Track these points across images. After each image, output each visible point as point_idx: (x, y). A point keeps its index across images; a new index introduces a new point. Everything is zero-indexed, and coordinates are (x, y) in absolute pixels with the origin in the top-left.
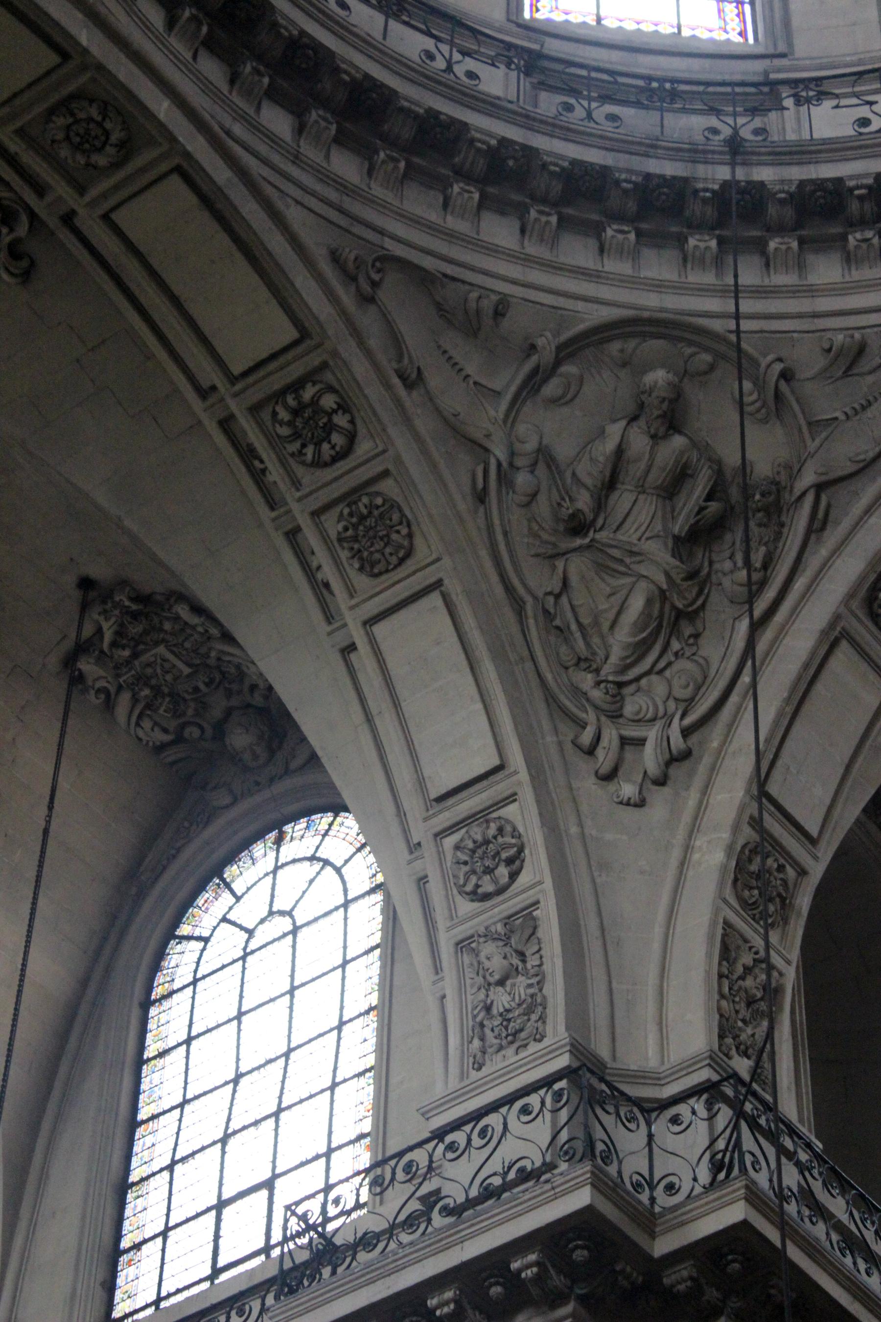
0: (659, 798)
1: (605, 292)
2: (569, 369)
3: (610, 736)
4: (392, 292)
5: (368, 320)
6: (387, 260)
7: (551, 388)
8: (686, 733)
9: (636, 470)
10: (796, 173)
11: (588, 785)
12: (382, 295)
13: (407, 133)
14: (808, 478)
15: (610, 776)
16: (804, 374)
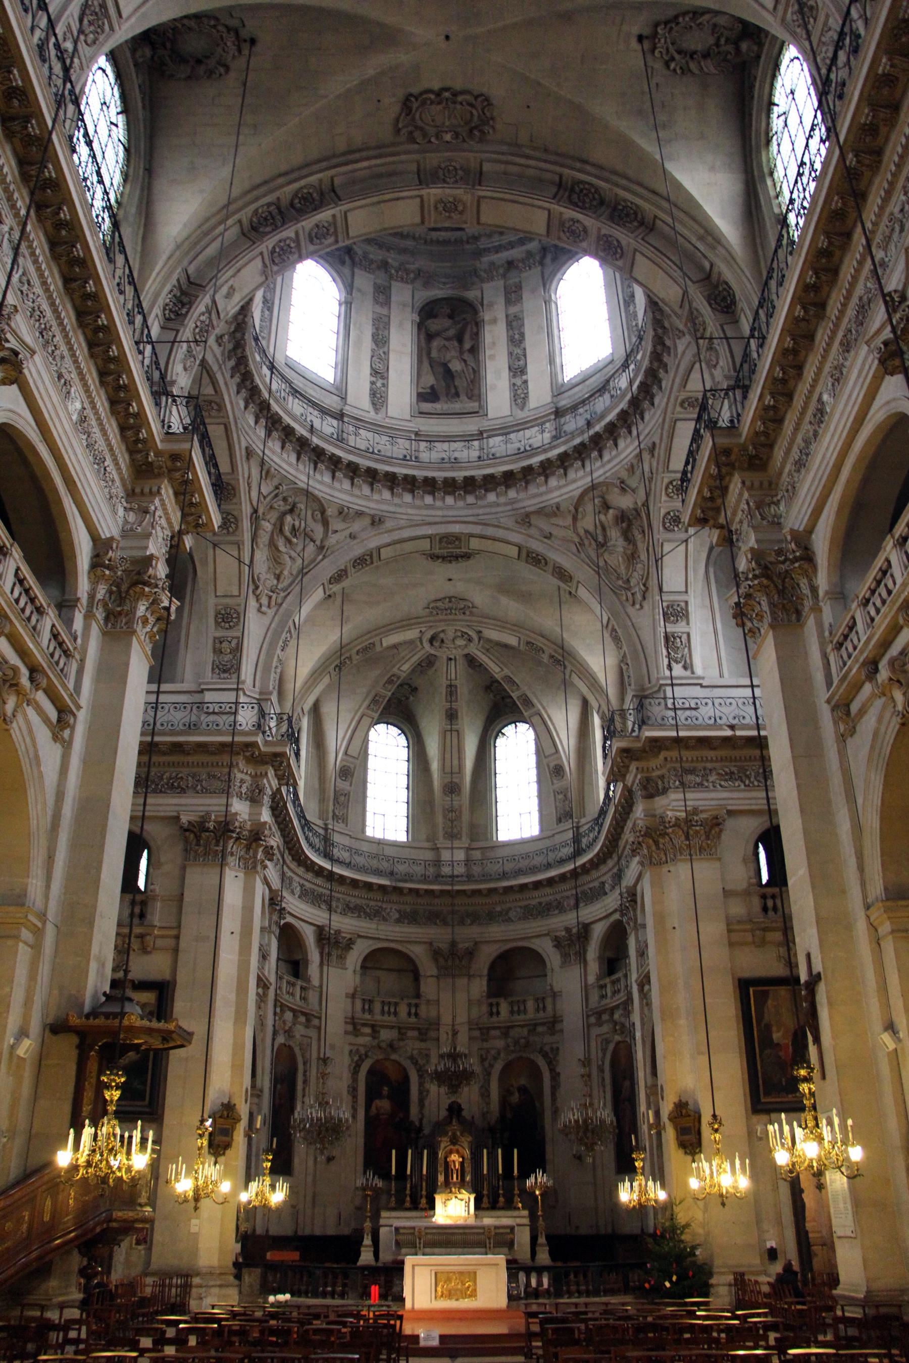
0: (645, 604)
1: (579, 484)
2: (580, 509)
3: (629, 594)
4: (534, 520)
5: (532, 531)
6: (528, 515)
7: (580, 516)
8: (644, 585)
9: (606, 524)
10: (603, 423)
11: (631, 610)
12: (533, 522)
13: (520, 476)
14: (640, 504)
15: (634, 604)
16: (625, 478)
